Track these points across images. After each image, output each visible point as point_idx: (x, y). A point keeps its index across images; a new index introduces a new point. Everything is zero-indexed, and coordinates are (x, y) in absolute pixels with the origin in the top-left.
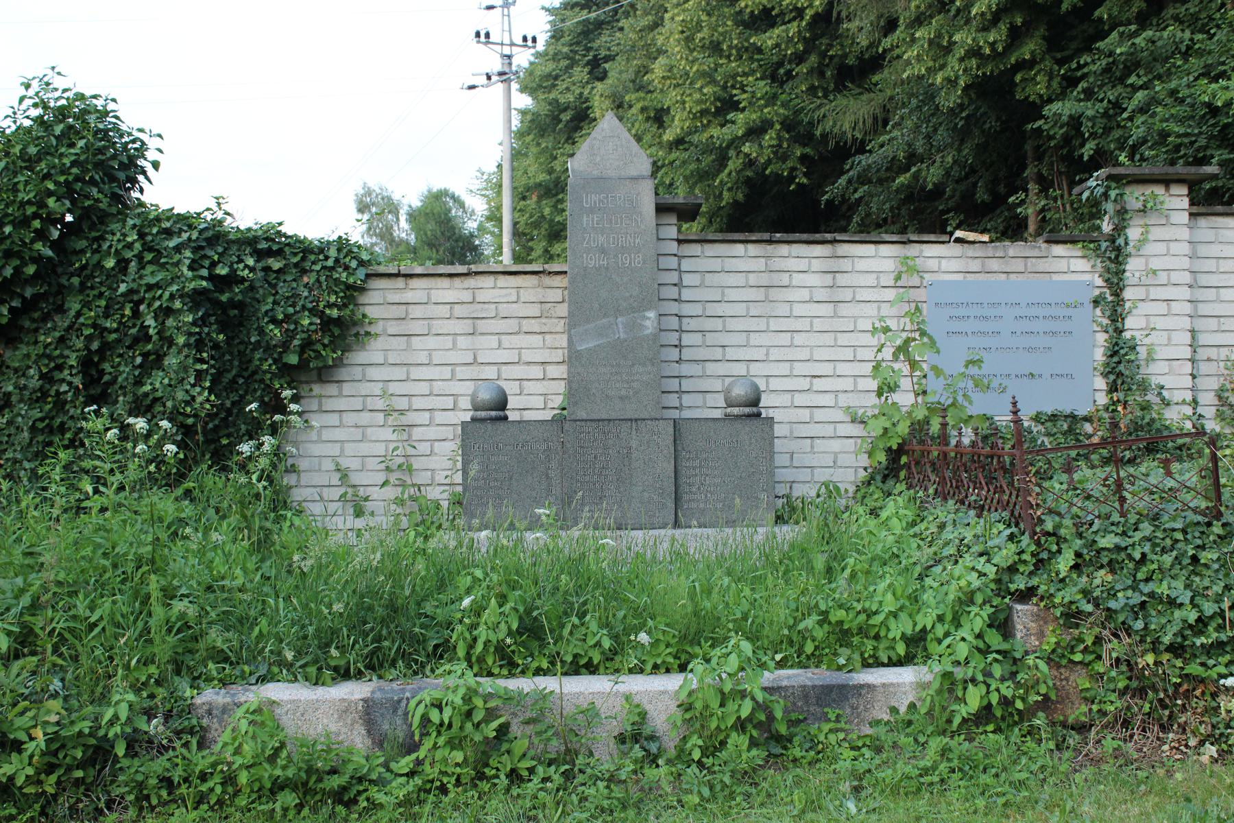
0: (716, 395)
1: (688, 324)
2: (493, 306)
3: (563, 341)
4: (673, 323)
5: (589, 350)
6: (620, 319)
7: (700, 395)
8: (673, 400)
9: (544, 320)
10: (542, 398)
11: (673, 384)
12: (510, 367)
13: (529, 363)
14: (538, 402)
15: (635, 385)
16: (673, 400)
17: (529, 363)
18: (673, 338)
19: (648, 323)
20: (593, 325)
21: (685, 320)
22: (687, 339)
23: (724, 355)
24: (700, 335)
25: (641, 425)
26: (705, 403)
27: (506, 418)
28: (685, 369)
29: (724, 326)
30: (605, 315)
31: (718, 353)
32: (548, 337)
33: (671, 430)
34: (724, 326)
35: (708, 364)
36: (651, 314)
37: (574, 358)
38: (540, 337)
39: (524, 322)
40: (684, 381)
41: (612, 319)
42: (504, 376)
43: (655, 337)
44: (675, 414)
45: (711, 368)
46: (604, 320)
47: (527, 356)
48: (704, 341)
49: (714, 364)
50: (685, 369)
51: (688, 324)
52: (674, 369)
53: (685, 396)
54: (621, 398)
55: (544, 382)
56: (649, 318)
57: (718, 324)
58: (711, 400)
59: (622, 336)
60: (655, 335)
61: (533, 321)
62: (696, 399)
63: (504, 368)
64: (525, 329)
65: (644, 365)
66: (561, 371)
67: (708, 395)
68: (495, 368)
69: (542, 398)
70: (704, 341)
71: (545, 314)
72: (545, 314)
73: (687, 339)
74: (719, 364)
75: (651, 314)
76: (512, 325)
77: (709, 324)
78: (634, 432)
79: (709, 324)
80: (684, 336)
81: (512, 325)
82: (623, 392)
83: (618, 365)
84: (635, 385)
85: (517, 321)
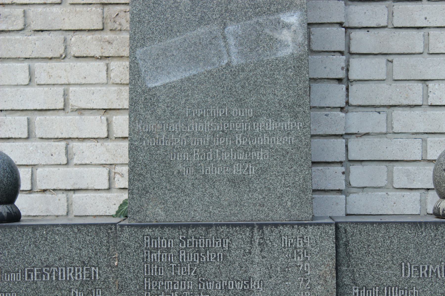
0: (410, 167)
1: (362, 41)
2: (19, 11)
3: (120, 70)
4: (336, 38)
5: (170, 87)
6: (231, 28)
7: (383, 167)
8: (333, 177)
9: (107, 36)
10: (105, 171)
11: (335, 149)
12: (49, 117)
13: (81, 111)
14: (100, 178)
15: (260, 155)
16: (333, 177)
17: (81, 111)
18: (334, 66)
19: (286, 36)
20: (178, 39)
21: (355, 35)
22: (359, 68)
23: (426, 96)
24: (383, 60)
25: (271, 235)
26: (391, 180)
27: (15, 217)
28: (356, 121)
29: (427, 45)
30: (202, 21)
31: (415, 94)
32: (114, 64)
33: (330, 245)
34: (427, 45)
35: (397, 112)
36: (293, 19)
37: (142, 102)
38: (102, 64)
39: (74, 38)
40: (353, 143)
41: (215, 27)
42: (39, 133)
43: (299, 63)
44: (335, 207)
45: (402, 120)
46: (201, 30)
47: (79, 98)
48: (390, 72)
49: (407, 112)
50: (356, 121)
51: (362, 41)
52: (337, 122)
53: (355, 170)
54: (234, 182)
55: (110, 144)
56: (288, 26)
57: (415, 42)
58: (401, 175)
59: (236, 60)
60: (299, 59)
61: (89, 37)
62: (379, 175)
63: (38, 118)
64: (74, 50)
65: (277, 117)
66: (121, 124)
67: (397, 167)
68: (23, 119)
69: (105, 171)
70: (390, 72)
71: (110, 25)
72: (110, 25)
73: (359, 68)
74: (417, 112)
75: (293, 19)
76: (51, 44)
77: (398, 42)
78: (257, 250)
79: (398, 42)
80: (355, 62)
81: (51, 44)
82: (237, 170)
83: (228, 118)
84: (260, 155)
85: (60, 37)
